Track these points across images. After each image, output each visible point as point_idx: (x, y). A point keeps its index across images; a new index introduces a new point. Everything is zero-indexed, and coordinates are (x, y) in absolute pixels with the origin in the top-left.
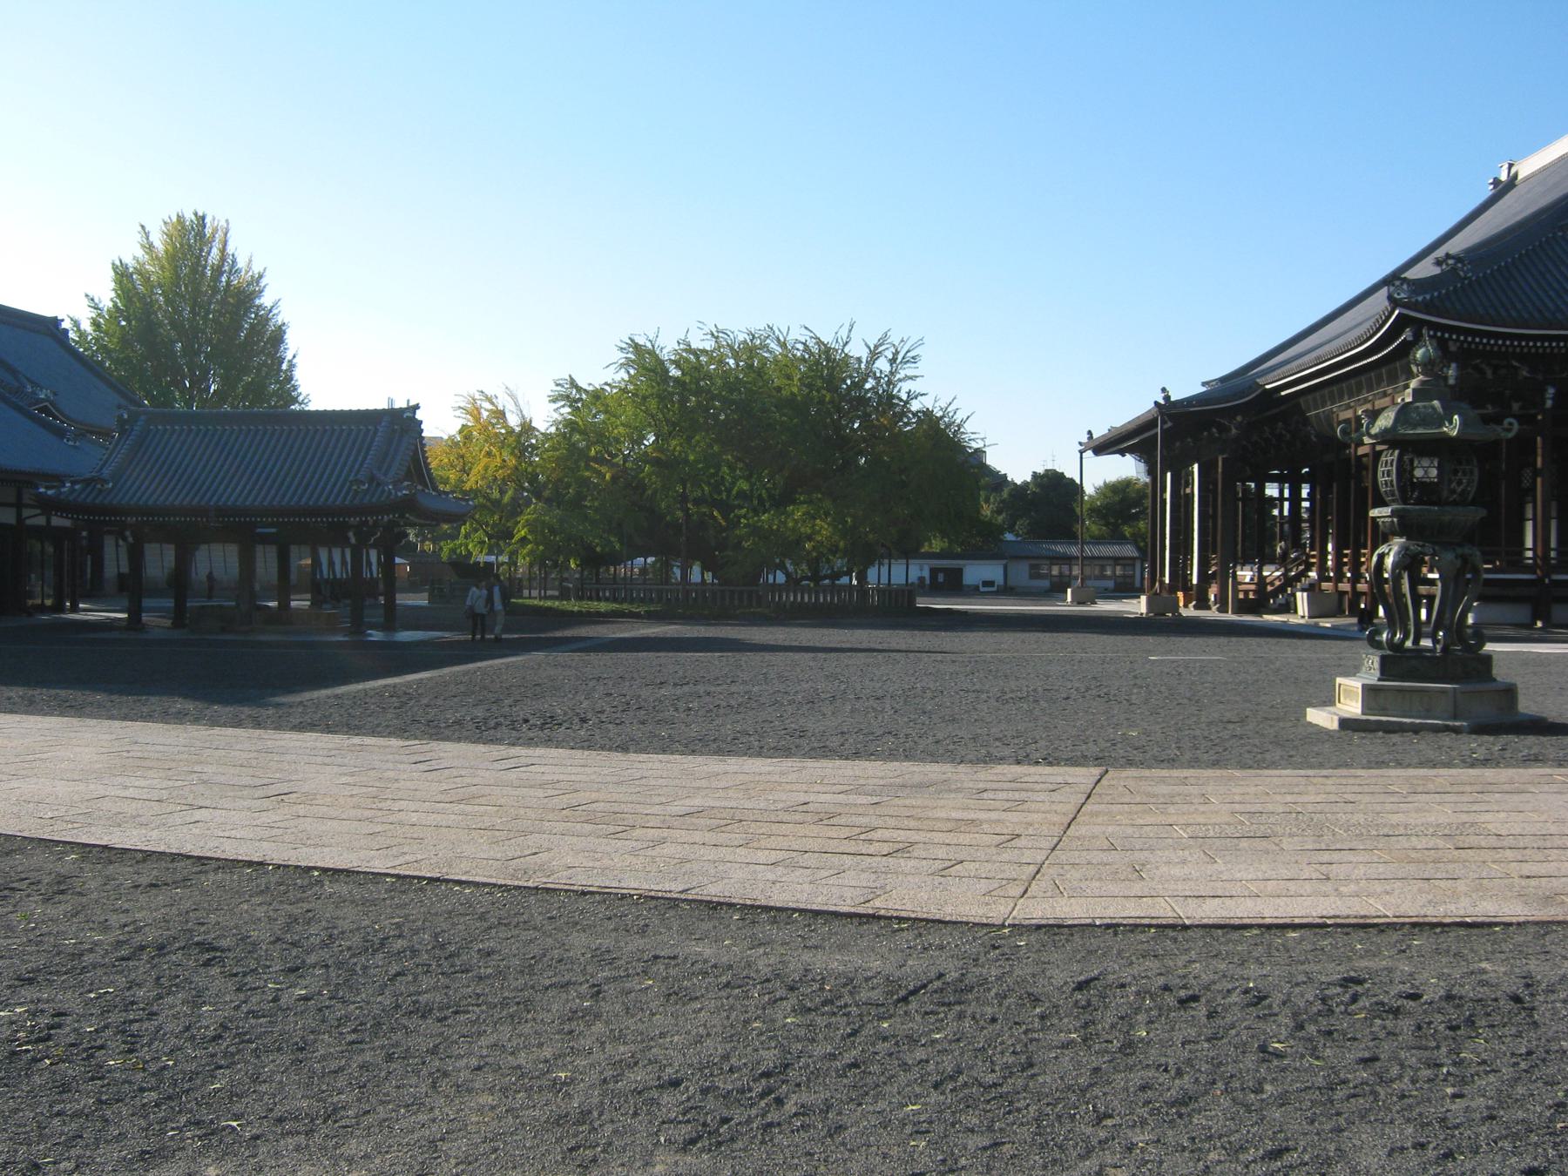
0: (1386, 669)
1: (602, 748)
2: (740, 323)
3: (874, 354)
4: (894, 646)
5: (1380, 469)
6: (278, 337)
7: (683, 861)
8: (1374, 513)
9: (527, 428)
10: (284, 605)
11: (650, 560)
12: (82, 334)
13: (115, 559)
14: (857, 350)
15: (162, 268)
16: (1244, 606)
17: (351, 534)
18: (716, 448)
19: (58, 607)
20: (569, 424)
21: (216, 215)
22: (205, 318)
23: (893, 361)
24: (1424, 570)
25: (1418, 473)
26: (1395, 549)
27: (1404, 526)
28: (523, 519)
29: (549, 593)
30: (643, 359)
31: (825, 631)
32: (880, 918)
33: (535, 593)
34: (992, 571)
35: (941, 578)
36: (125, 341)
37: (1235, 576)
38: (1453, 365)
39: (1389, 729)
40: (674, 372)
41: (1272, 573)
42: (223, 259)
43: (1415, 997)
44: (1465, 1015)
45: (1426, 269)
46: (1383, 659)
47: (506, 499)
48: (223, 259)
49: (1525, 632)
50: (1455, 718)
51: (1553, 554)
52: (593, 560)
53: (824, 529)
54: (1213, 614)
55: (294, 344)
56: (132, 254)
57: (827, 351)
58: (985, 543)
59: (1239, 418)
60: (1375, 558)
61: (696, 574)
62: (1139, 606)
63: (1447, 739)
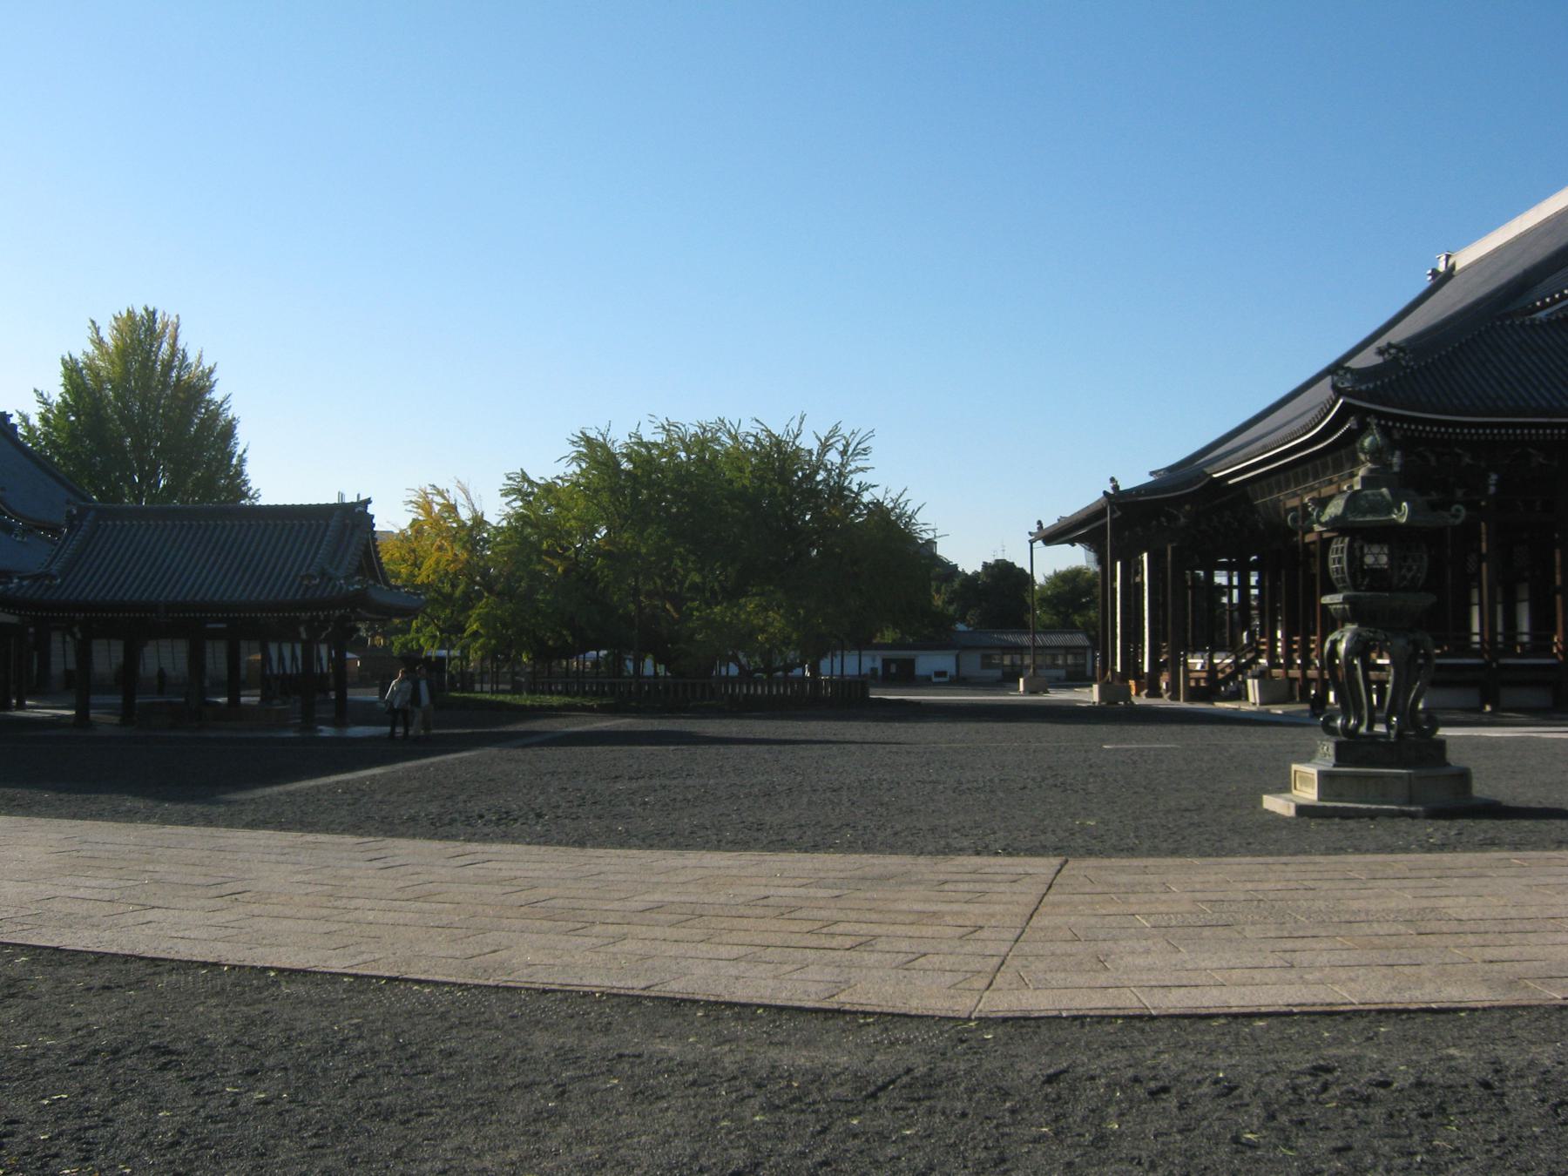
0: (1342, 756)
1: (559, 843)
2: (692, 416)
3: (825, 447)
4: (848, 737)
5: (1332, 556)
6: (229, 431)
7: (645, 957)
8: (1326, 600)
9: (479, 522)
10: (234, 700)
11: (603, 653)
12: (31, 429)
13: (62, 657)
14: (808, 442)
15: (112, 363)
16: (1195, 694)
17: (302, 629)
18: (668, 541)
19: (8, 707)
20: (520, 517)
21: (167, 310)
22: (155, 413)
23: (843, 453)
24: (1374, 655)
25: (1369, 560)
26: (1348, 635)
27: (1356, 612)
28: (474, 613)
29: (501, 687)
30: (595, 452)
31: (779, 723)
32: (845, 1012)
33: (487, 687)
34: (943, 661)
35: (893, 669)
36: (74, 437)
37: (1186, 664)
38: (1398, 453)
39: (1345, 814)
40: (626, 465)
41: (1223, 660)
42: (173, 354)
43: (1385, 1084)
44: (1435, 1101)
45: (1369, 359)
46: (1338, 746)
47: (458, 593)
48: (173, 354)
49: (1475, 717)
50: (1411, 803)
51: (1500, 638)
52: (544, 654)
53: (777, 621)
54: (1164, 702)
55: (244, 438)
56: (81, 348)
57: (778, 443)
58: (938, 635)
59: (1187, 507)
60: (1327, 645)
61: (648, 667)
62: (1092, 695)
63: (1403, 824)
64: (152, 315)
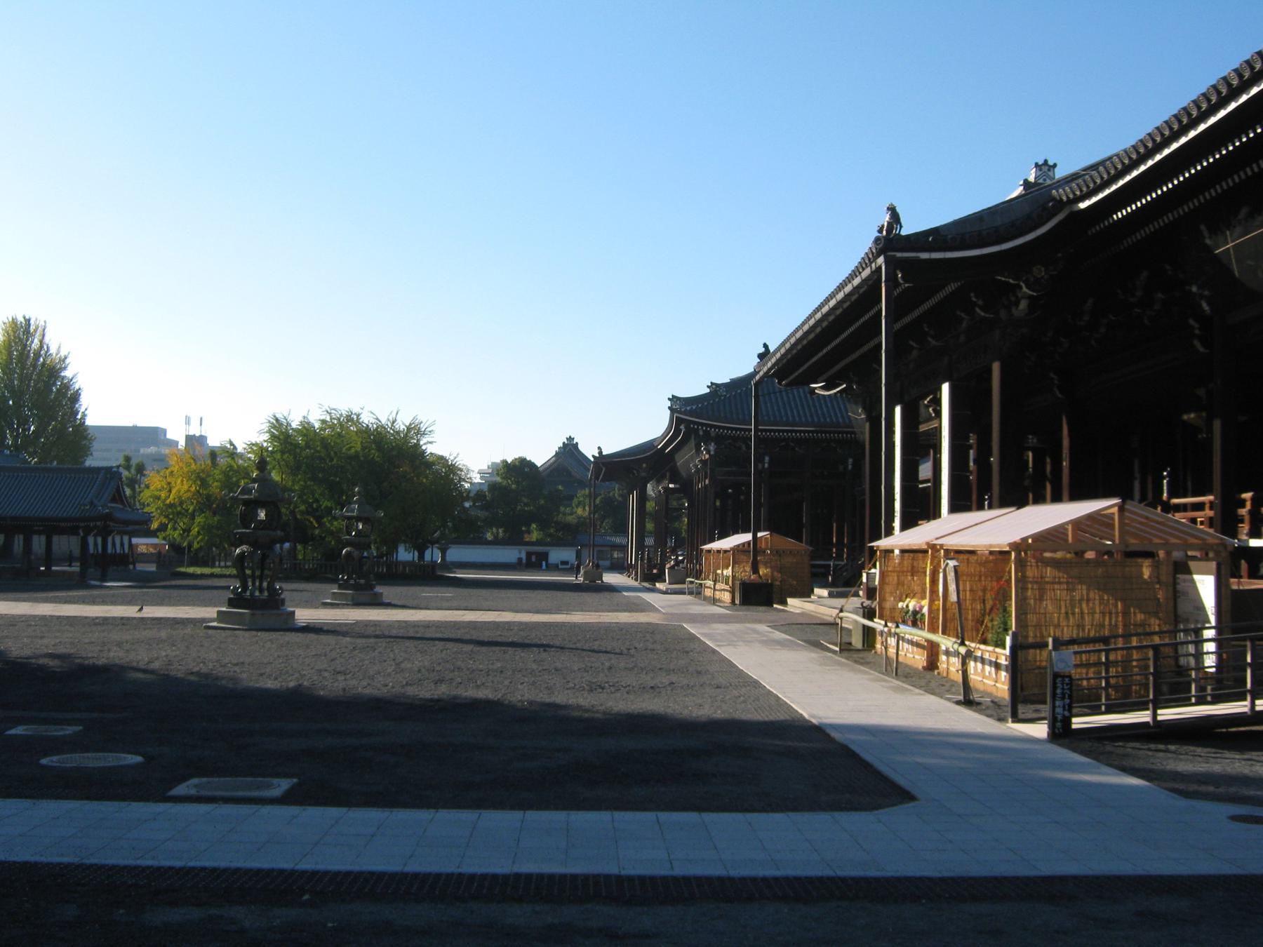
3: (409, 429)
6: (76, 397)
10: (48, 568)
21: (37, 314)
22: (29, 386)
33: (222, 564)
34: (568, 554)
35: (534, 558)
42: (41, 347)
48: (41, 347)
58: (569, 535)
64: (28, 321)
